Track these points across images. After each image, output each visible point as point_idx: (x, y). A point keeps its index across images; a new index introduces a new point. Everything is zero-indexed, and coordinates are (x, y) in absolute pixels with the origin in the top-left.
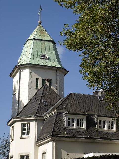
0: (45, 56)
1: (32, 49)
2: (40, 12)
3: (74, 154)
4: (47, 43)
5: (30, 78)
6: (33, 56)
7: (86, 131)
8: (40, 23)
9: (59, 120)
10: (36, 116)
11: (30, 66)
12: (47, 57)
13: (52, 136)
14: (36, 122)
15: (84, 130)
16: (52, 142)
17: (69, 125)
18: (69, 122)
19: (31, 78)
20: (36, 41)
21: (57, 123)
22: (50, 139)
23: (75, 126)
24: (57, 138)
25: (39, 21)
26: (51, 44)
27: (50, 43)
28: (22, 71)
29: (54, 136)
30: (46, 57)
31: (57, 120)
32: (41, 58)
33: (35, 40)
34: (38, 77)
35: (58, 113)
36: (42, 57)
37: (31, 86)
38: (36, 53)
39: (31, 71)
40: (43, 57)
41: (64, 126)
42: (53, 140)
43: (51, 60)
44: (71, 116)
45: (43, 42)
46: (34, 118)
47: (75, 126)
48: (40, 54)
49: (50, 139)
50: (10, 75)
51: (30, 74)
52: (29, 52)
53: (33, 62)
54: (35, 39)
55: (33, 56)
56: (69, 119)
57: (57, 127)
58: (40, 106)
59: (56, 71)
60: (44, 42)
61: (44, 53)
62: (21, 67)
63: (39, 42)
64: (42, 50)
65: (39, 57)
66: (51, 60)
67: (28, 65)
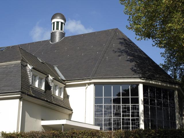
3: (35, 119)
13: (22, 93)
16: (18, 100)
22: (19, 95)
24: (26, 97)
41: (28, 82)
42: (20, 98)
44: (37, 73)
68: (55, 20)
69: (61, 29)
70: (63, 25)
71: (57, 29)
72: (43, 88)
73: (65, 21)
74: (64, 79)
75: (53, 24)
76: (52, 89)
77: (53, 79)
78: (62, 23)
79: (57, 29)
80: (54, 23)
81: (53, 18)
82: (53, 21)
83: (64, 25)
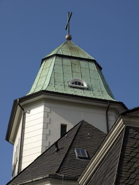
1: (52, 68)
2: (69, 21)
4: (82, 63)
5: (47, 124)
6: (54, 80)
8: (69, 39)
11: (48, 97)
12: (85, 85)
19: (50, 123)
20: (59, 60)
21: (129, 161)
25: (67, 36)
26: (93, 66)
27: (90, 63)
28: (29, 113)
30: (83, 85)
31: (128, 151)
32: (71, 87)
33: (58, 57)
34: (65, 122)
35: (131, 131)
36: (73, 84)
37: (48, 141)
38: (61, 78)
39: (49, 110)
40: (77, 84)
43: (93, 90)
45: (74, 61)
48: (70, 79)
50: (7, 139)
51: (46, 116)
52: (45, 78)
53: (51, 89)
54: (57, 55)
57: (133, 176)
58: (68, 159)
59: (107, 112)
60: (77, 61)
61: (78, 78)
62: (24, 103)
63: (66, 61)
64: (74, 74)
65: (66, 84)
66: (93, 90)
67: (42, 96)
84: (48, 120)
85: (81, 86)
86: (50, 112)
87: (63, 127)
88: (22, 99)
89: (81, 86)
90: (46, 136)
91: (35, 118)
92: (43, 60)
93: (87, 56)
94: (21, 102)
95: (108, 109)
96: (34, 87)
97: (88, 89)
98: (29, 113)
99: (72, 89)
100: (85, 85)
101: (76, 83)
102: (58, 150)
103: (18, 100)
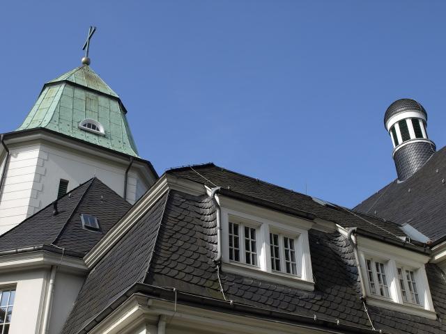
0: (94, 127)
1: (57, 98)
2: (90, 38)
4: (102, 100)
5: (40, 176)
7: (318, 298)
8: (87, 63)
9: (182, 224)
10: (48, 250)
11: (46, 137)
14: (47, 279)
15: (305, 287)
17: (235, 255)
18: (234, 242)
20: (70, 89)
21: (171, 237)
22: (136, 309)
23: (263, 262)
25: (83, 59)
26: (115, 106)
29: (156, 294)
30: (98, 130)
31: (170, 223)
32: (82, 129)
33: (68, 85)
34: (66, 178)
36: (85, 125)
40: (91, 127)
43: (111, 139)
45: (91, 94)
46: (41, 259)
47: (263, 262)
48: (82, 119)
49: (136, 309)
51: (41, 164)
52: (45, 111)
53: (52, 128)
54: (68, 82)
55: (56, 118)
56: (234, 228)
57: (175, 257)
58: (71, 227)
59: (127, 172)
60: (95, 95)
61: (92, 118)
64: (88, 112)
65: (75, 124)
66: (111, 139)
67: (39, 135)
68: (393, 121)
69: (418, 134)
70: (421, 124)
71: (406, 136)
72: (304, 272)
73: (423, 111)
74: (425, 239)
75: (391, 133)
76: (360, 278)
77: (353, 232)
78: (415, 121)
79: (406, 136)
80: (393, 129)
81: (388, 116)
82: (389, 125)
83: (425, 124)
84: (42, 171)
85: (96, 131)
86: (47, 160)
87: (64, 184)
88: (7, 136)
89: (96, 131)
90: (37, 192)
91: (25, 165)
92: (46, 86)
93: (109, 91)
94: (6, 139)
95: (129, 168)
96: (28, 120)
97: (104, 136)
98: (16, 157)
99: (82, 133)
100: (102, 131)
101: (89, 126)
102: (57, 213)
103: (2, 136)
